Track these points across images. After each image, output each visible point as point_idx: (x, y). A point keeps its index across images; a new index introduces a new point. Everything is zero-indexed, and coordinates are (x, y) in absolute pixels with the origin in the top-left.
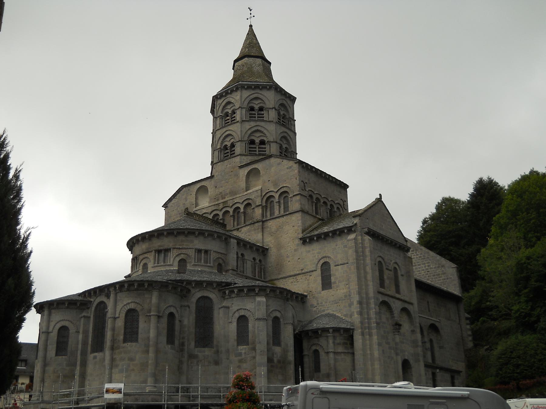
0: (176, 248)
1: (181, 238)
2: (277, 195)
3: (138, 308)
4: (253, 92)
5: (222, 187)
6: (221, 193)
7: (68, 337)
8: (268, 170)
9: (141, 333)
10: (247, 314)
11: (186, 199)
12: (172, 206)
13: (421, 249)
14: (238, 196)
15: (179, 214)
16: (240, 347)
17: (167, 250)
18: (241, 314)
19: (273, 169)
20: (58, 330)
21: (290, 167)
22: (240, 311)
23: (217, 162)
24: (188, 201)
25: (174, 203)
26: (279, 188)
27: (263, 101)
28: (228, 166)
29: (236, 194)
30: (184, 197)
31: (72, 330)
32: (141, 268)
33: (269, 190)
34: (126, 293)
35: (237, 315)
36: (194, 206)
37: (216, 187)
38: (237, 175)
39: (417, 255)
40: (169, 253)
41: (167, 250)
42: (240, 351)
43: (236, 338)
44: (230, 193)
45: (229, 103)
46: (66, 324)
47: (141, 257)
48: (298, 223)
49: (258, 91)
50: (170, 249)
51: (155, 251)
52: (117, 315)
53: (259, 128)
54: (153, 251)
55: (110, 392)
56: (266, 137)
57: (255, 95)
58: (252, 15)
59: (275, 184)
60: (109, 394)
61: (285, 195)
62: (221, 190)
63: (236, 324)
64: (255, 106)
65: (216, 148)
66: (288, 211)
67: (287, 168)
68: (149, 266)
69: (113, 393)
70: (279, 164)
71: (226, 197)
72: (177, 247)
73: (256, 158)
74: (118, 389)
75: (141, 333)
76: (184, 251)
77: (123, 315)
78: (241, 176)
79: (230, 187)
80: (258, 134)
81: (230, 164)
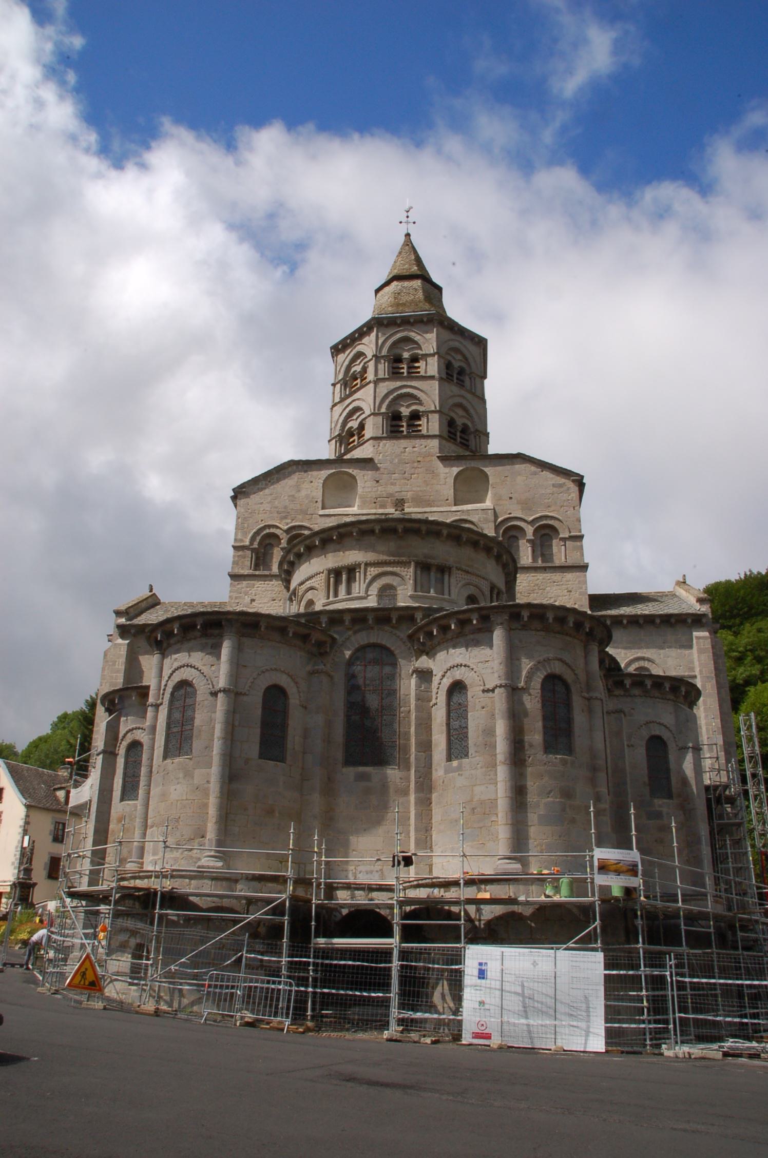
0: (462, 570)
1: (468, 551)
2: (530, 527)
3: (569, 677)
4: (453, 337)
5: (392, 484)
7: (285, 713)
8: (508, 479)
9: (579, 736)
10: (666, 735)
11: (298, 488)
14: (435, 509)
15: (278, 512)
16: (657, 802)
17: (443, 570)
18: (653, 733)
19: (519, 479)
20: (263, 691)
21: (561, 486)
22: (651, 725)
23: (380, 435)
24: (303, 493)
26: (537, 515)
27: (466, 359)
31: (294, 700)
32: (376, 593)
33: (510, 514)
34: (538, 633)
35: (645, 734)
36: (320, 505)
37: (378, 482)
40: (446, 577)
41: (443, 570)
42: (657, 809)
43: (646, 779)
46: (283, 681)
47: (372, 571)
48: (581, 588)
49: (459, 338)
50: (450, 569)
51: (417, 564)
52: (522, 684)
53: (465, 402)
54: (412, 563)
55: (610, 871)
56: (473, 422)
57: (456, 344)
58: (411, 220)
60: (609, 876)
61: (543, 532)
62: (391, 489)
63: (644, 752)
64: (453, 362)
65: (379, 410)
66: (552, 561)
67: (554, 485)
68: (399, 592)
69: (619, 875)
70: (535, 473)
72: (464, 567)
74: (629, 866)
75: (579, 736)
76: (475, 580)
77: (537, 684)
78: (442, 476)
79: (414, 489)
80: (461, 412)
81: (414, 447)
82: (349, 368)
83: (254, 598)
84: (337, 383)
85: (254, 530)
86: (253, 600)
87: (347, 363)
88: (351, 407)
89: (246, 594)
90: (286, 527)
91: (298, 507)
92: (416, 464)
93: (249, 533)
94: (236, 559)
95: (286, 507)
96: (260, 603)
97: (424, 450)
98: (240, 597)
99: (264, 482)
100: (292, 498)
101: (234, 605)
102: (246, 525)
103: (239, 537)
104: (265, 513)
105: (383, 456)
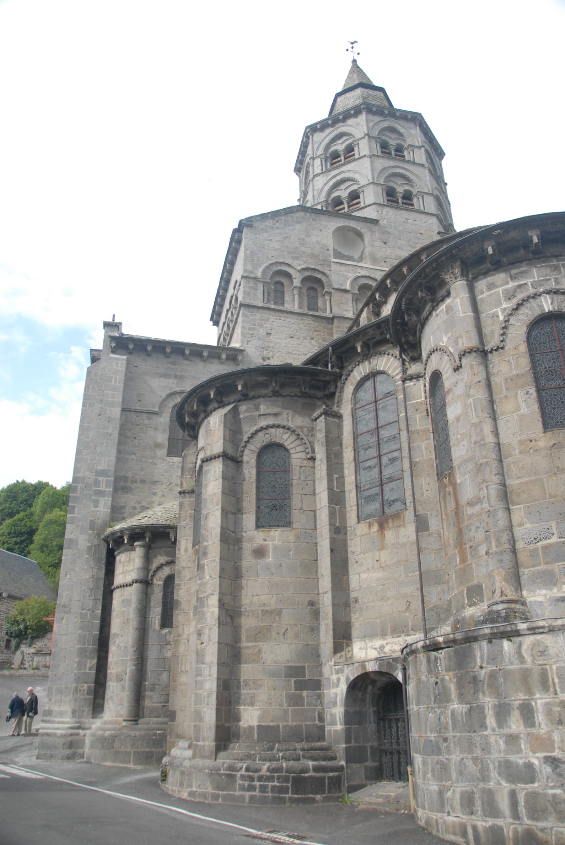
5: (399, 248)
15: (288, 252)
45: (393, 130)
81: (415, 220)
82: (328, 146)
83: (270, 331)
84: (317, 157)
85: (265, 265)
86: (269, 334)
87: (327, 140)
88: (338, 178)
89: (261, 326)
90: (299, 268)
91: (309, 251)
92: (419, 235)
93: (260, 266)
94: (247, 289)
95: (296, 248)
96: (278, 338)
97: (425, 225)
98: (254, 329)
99: (271, 221)
100: (303, 242)
101: (248, 336)
102: (255, 258)
103: (249, 268)
104: (277, 251)
105: (387, 221)
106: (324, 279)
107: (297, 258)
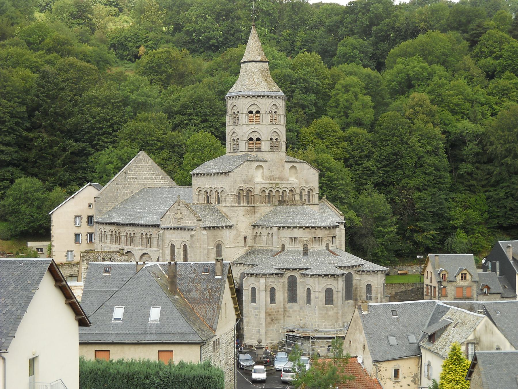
6: (273, 176)
12: (236, 173)
13: (168, 178)
21: (315, 174)
25: (238, 171)
26: (309, 186)
28: (277, 157)
29: (282, 180)
30: (246, 169)
38: (283, 166)
39: (165, 182)
44: (279, 178)
59: (306, 183)
62: (273, 173)
70: (308, 169)
71: (276, 180)
73: (301, 161)
78: (286, 168)
89: (236, 213)
106: (252, 190)
107: (245, 183)
